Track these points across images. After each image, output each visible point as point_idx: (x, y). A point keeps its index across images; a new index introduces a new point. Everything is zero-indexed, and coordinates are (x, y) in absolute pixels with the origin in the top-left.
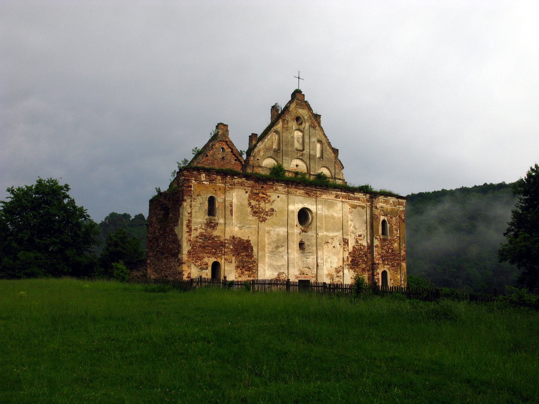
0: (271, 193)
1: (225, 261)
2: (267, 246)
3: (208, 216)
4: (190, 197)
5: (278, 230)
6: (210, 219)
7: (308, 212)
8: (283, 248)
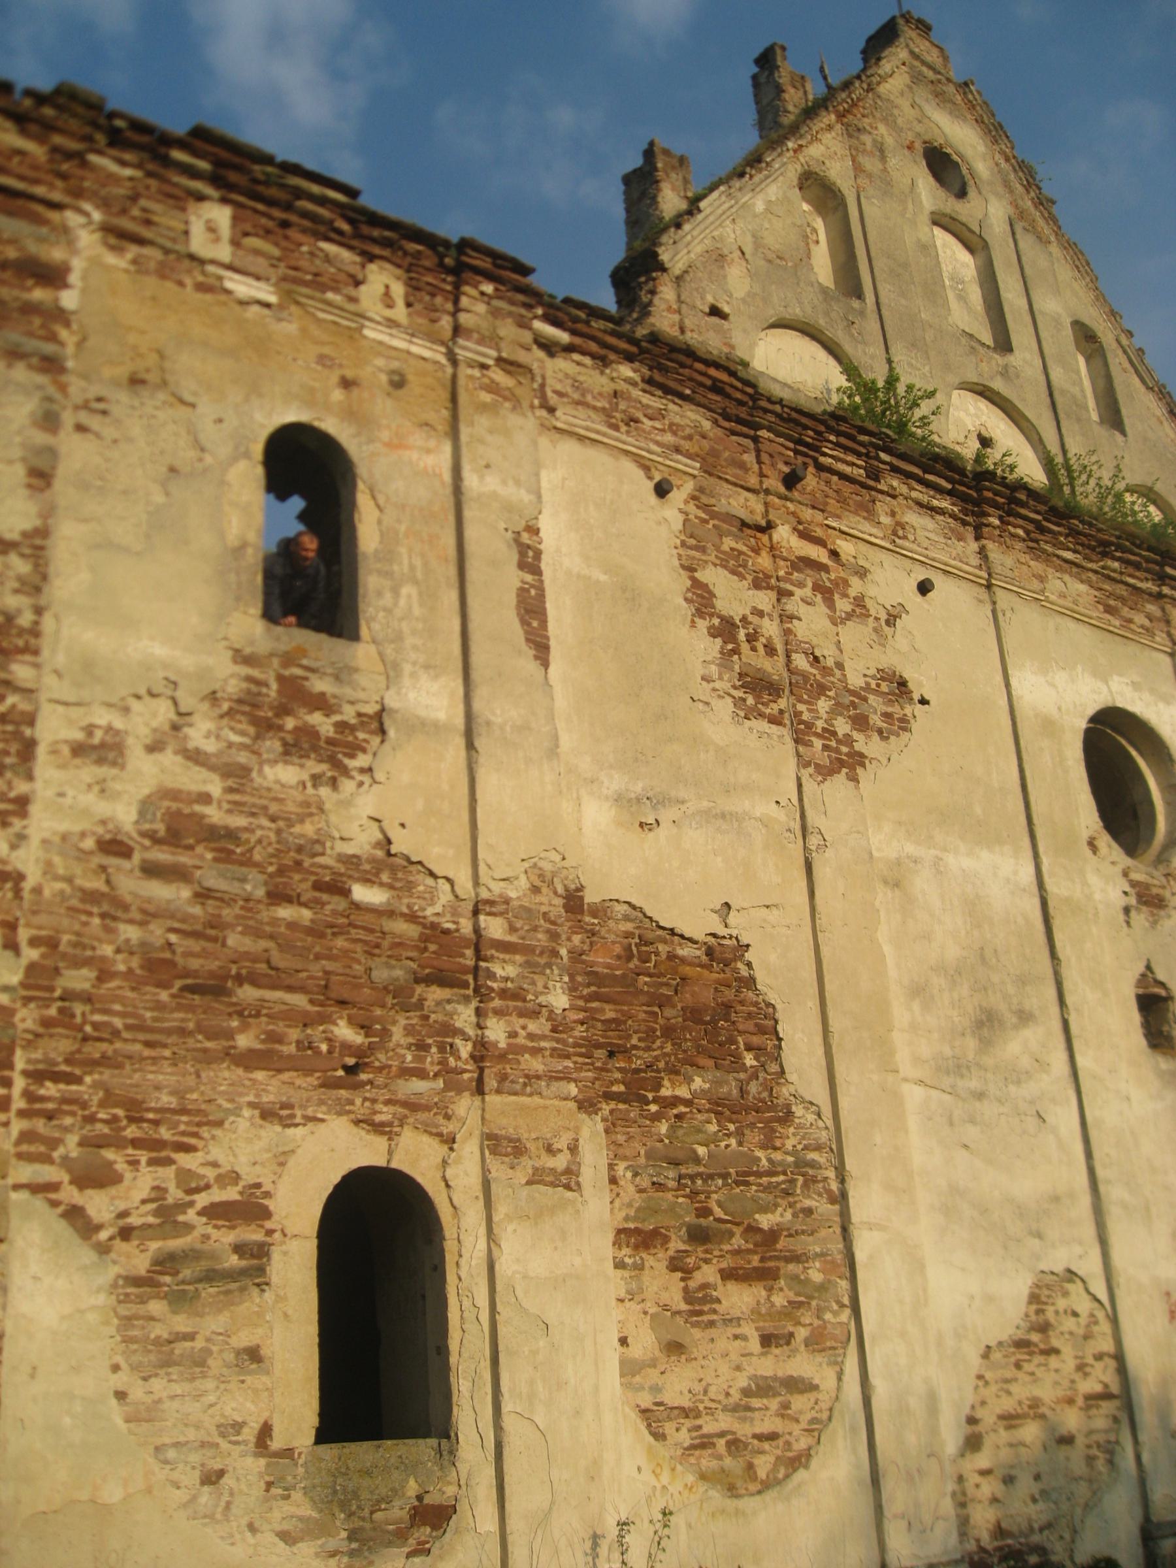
0: (863, 547)
1: (498, 1169)
2: (901, 1013)
3: (269, 616)
4: (41, 379)
5: (967, 863)
6: (288, 659)
7: (1134, 753)
8: (1031, 1035)
